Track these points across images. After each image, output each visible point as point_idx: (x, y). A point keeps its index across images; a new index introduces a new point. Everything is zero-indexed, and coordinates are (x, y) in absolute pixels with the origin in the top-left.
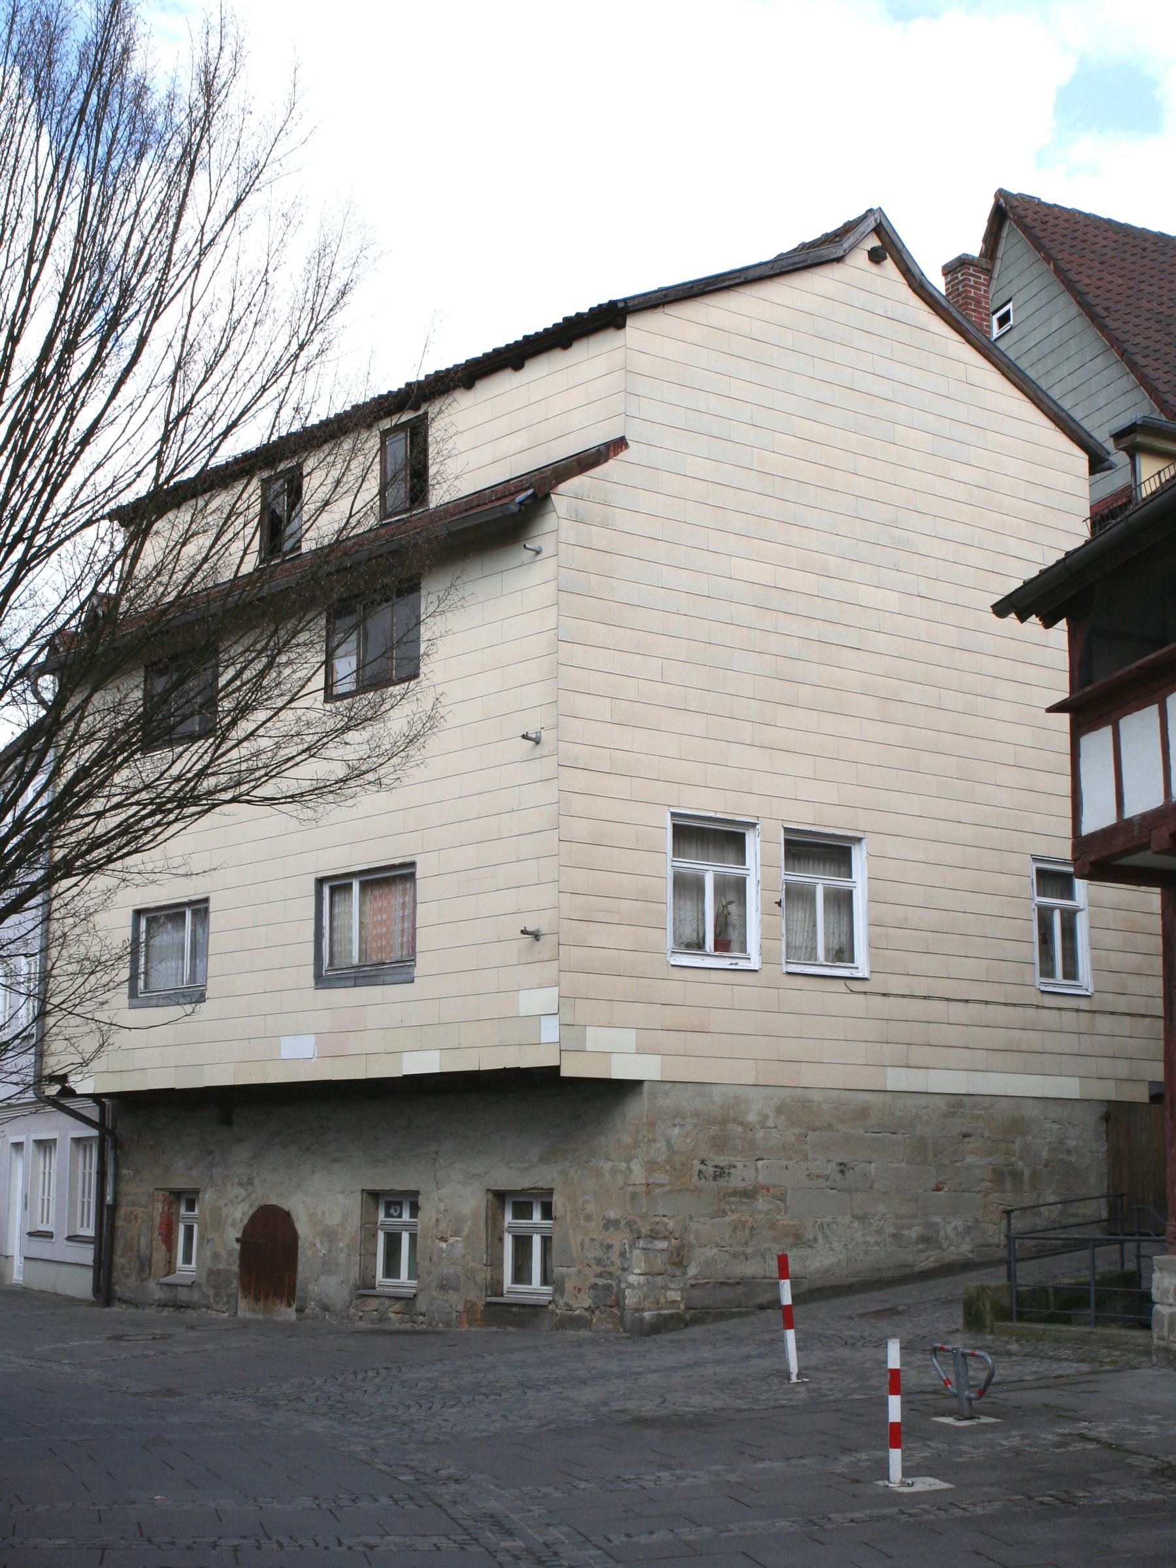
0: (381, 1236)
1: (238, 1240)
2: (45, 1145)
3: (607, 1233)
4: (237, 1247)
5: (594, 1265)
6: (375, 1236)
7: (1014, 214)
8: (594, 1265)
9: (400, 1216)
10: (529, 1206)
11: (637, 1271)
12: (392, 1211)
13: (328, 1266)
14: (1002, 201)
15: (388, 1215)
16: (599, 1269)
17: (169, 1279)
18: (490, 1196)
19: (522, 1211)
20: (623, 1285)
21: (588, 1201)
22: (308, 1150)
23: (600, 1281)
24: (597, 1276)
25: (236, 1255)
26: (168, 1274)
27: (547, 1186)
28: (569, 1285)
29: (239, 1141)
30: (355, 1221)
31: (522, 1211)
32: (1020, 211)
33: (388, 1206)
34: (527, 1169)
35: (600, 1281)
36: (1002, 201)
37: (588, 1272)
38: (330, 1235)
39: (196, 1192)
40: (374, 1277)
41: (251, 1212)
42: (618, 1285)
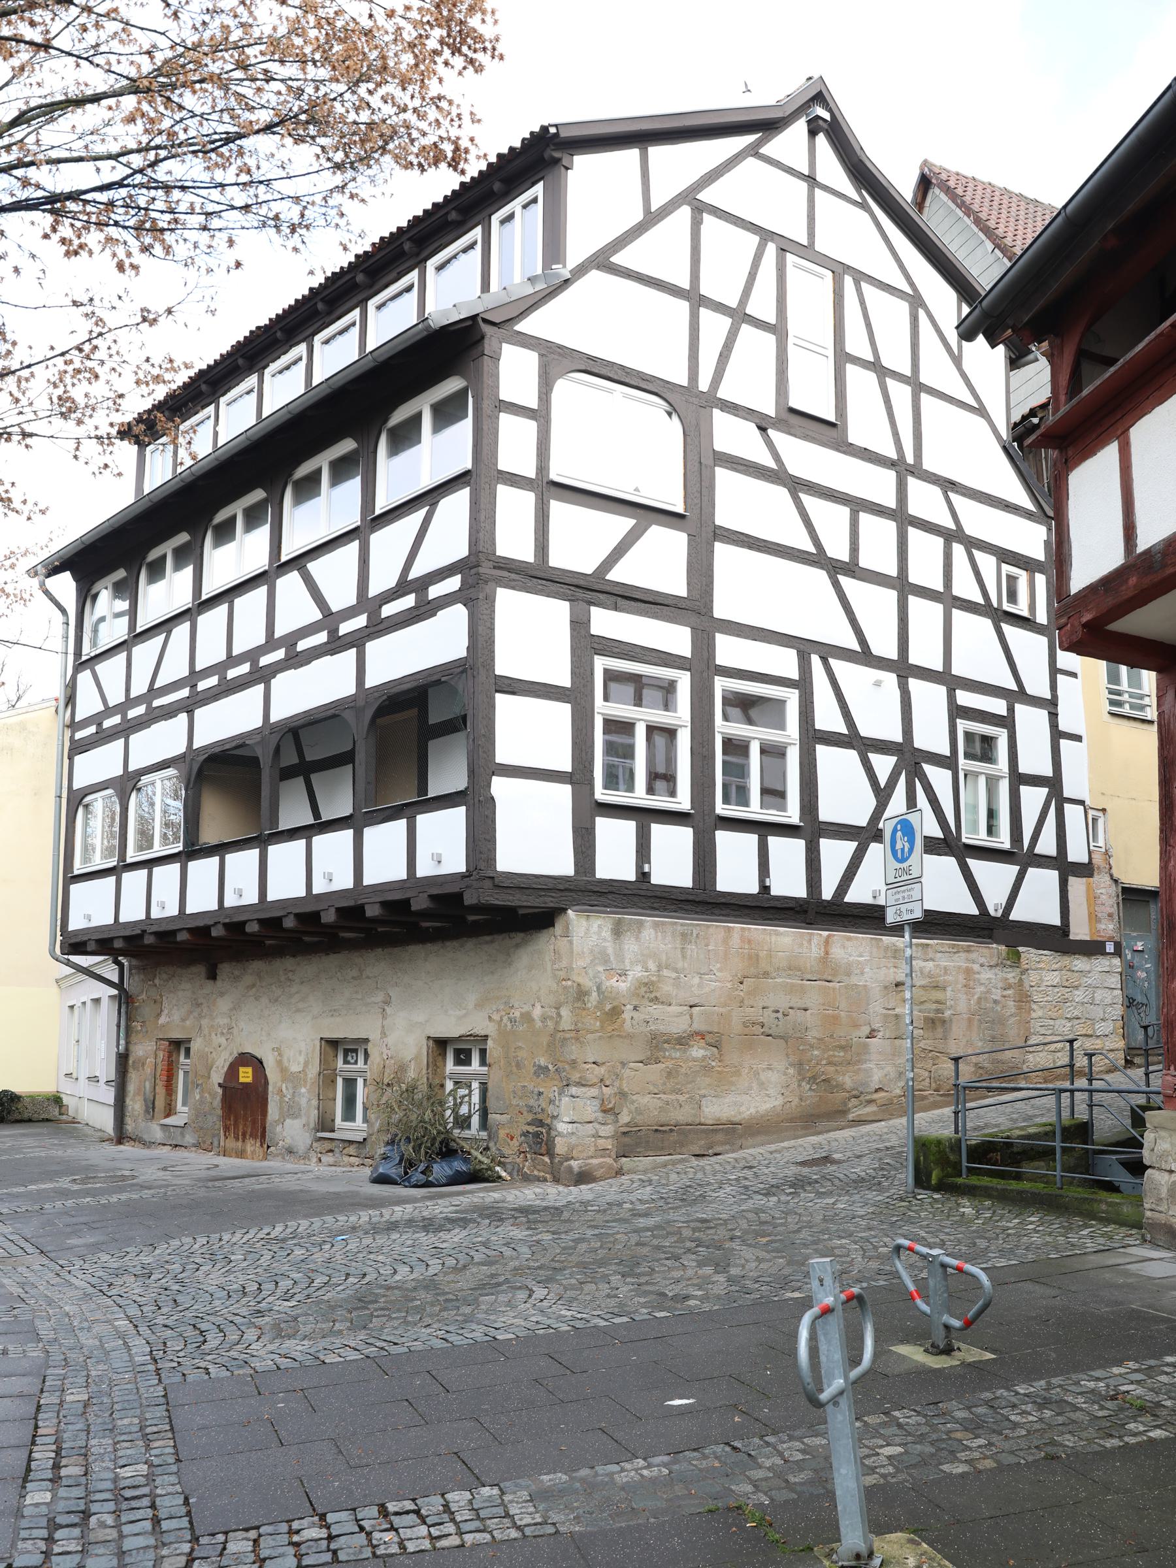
0: (340, 1081)
1: (220, 1085)
2: (97, 1001)
3: (539, 1080)
4: (220, 1091)
5: (525, 1113)
6: (334, 1082)
7: (937, 179)
8: (525, 1113)
9: (356, 1063)
10: (468, 1053)
11: (567, 1119)
12: (349, 1058)
13: (292, 1111)
14: (926, 170)
15: (346, 1062)
16: (530, 1118)
17: (168, 1121)
18: (431, 1043)
19: (463, 1058)
20: (553, 1133)
21: (520, 1048)
22: (276, 1000)
23: (531, 1129)
24: (529, 1124)
25: (219, 1098)
26: (168, 1115)
27: (483, 1033)
28: (502, 1133)
29: (222, 994)
30: (314, 1070)
31: (463, 1058)
32: (944, 176)
33: (346, 1052)
34: (465, 1016)
35: (531, 1129)
36: (926, 170)
37: (521, 1119)
38: (295, 1080)
39: (189, 1041)
40: (333, 1121)
41: (231, 1060)
42: (548, 1133)
